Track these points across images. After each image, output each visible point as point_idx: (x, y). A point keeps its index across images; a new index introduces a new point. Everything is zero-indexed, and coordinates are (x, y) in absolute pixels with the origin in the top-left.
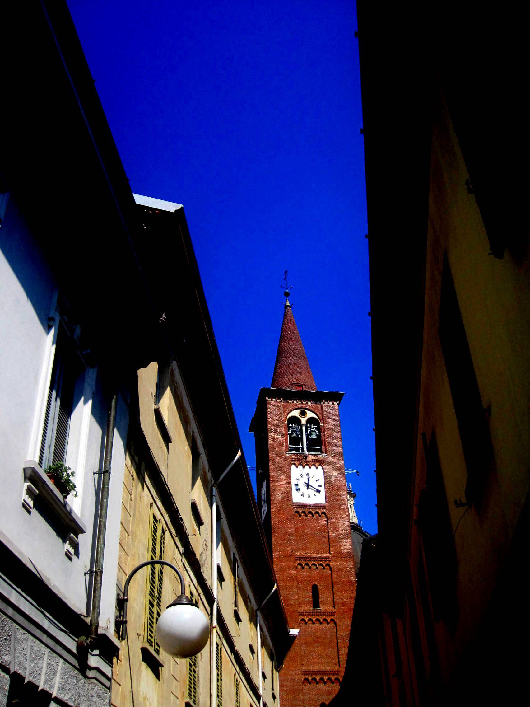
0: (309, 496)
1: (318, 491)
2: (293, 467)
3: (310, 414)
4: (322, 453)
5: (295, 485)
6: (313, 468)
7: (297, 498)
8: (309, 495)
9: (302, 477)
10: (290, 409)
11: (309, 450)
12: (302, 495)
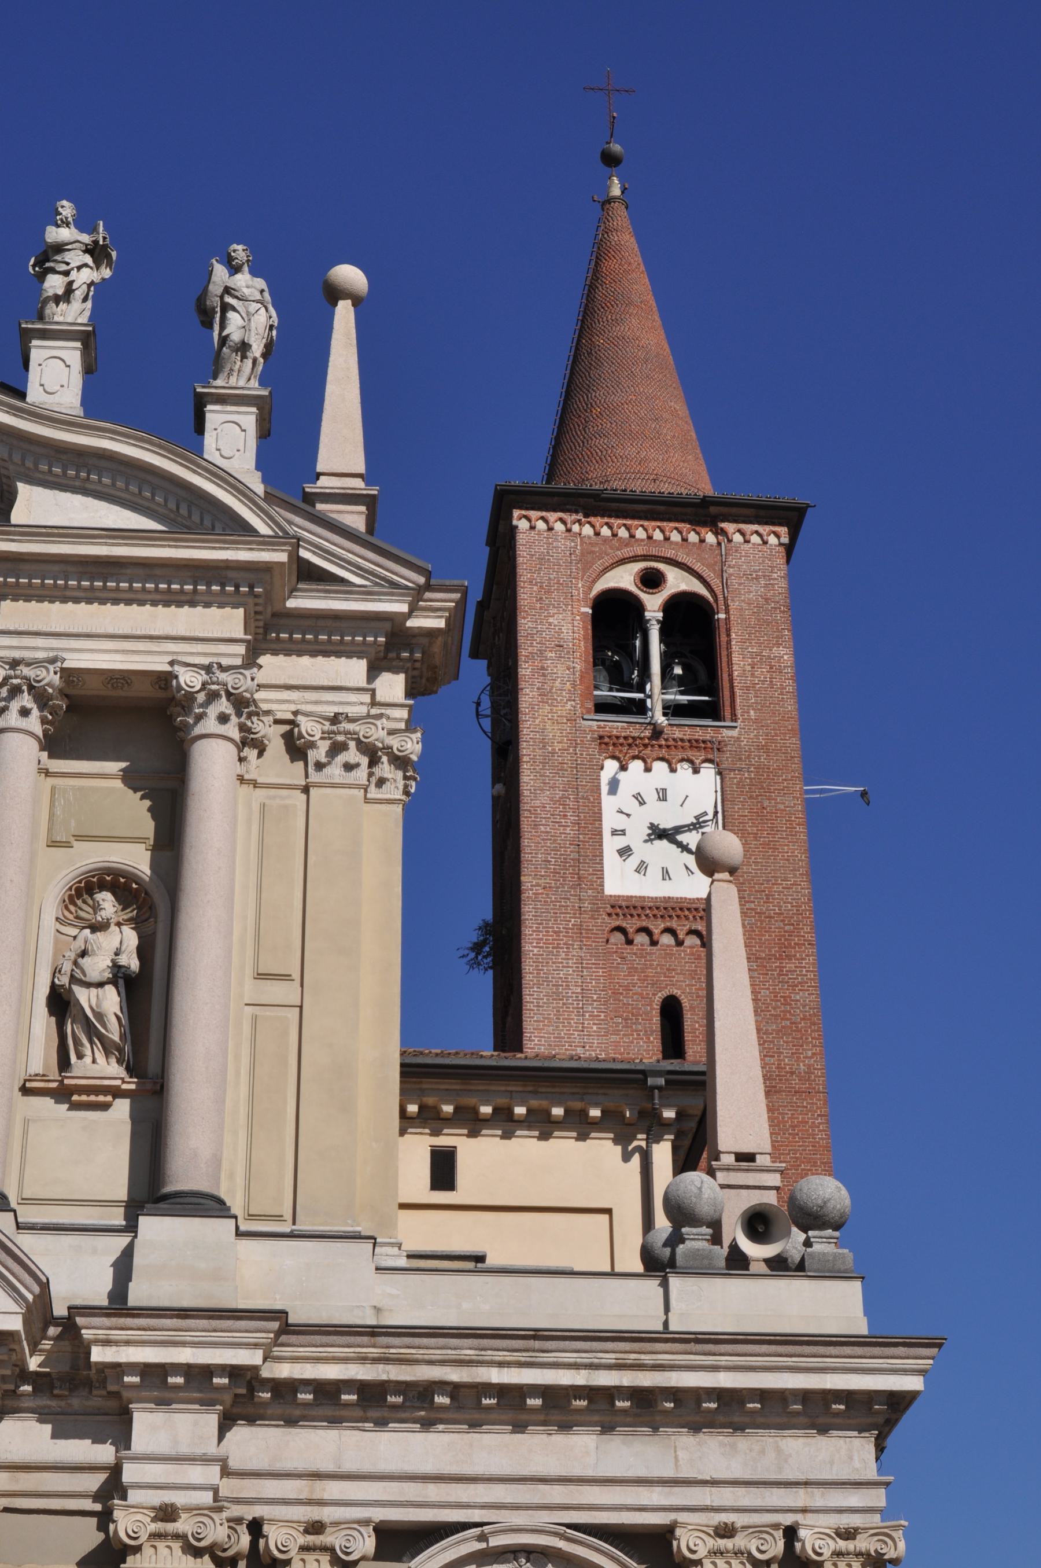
0: (666, 874)
3: (677, 582)
4: (719, 720)
5: (615, 833)
6: (684, 770)
8: (667, 872)
9: (642, 803)
10: (608, 561)
11: (673, 710)
12: (637, 871)
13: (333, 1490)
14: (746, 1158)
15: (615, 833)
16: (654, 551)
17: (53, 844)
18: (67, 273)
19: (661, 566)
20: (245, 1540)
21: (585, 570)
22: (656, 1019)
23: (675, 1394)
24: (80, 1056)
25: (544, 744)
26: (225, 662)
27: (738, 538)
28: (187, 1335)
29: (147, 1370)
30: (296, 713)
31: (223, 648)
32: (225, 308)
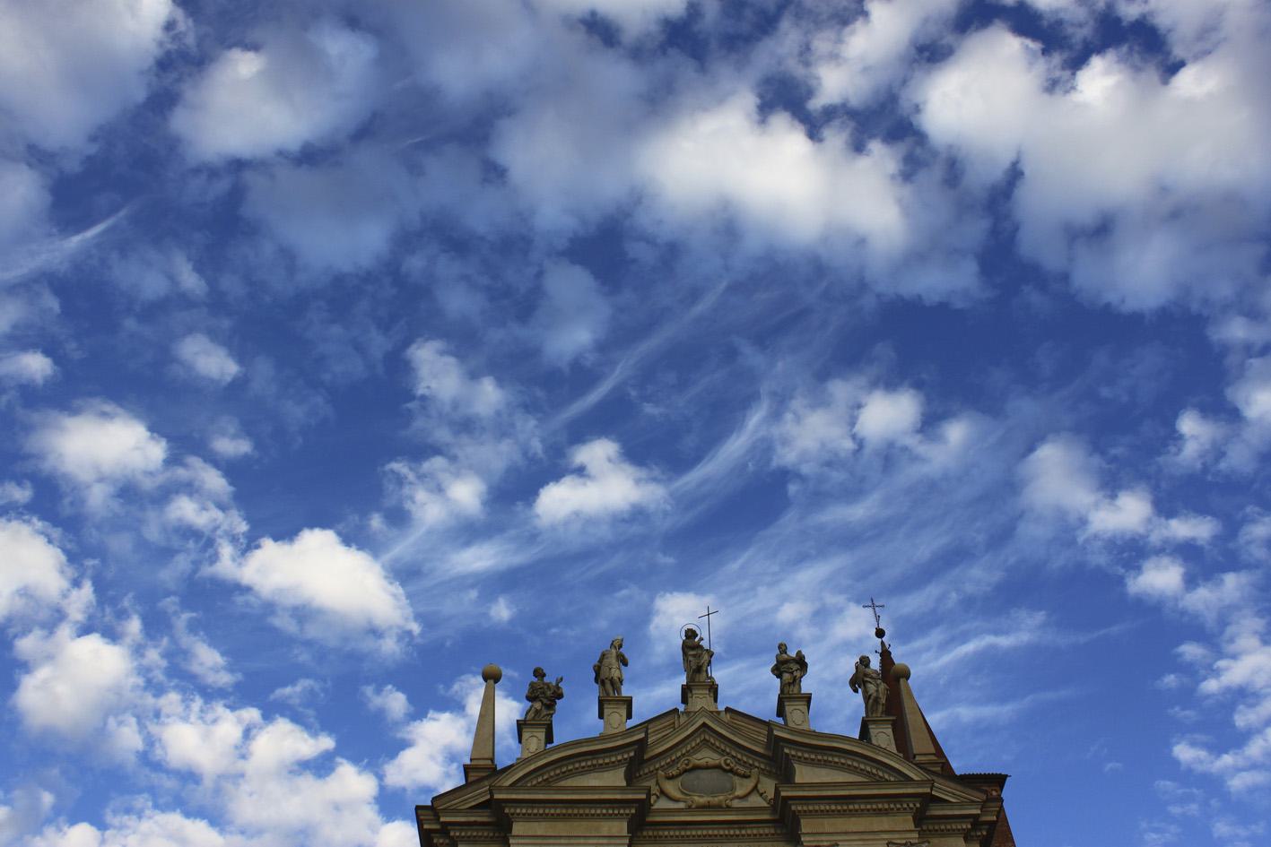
18: (792, 673)
31: (908, 835)
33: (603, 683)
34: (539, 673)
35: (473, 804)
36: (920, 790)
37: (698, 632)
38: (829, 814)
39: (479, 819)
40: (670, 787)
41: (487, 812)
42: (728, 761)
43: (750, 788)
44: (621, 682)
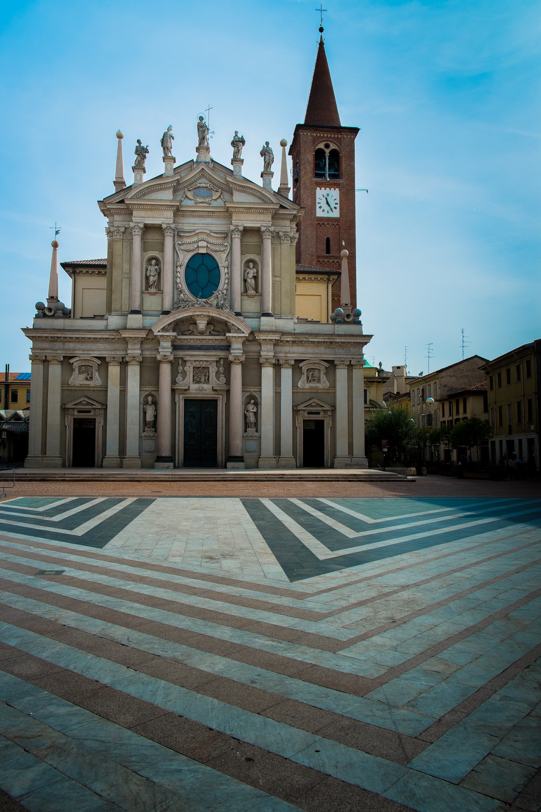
1: (335, 208)
2: (318, 188)
3: (333, 146)
5: (318, 203)
6: (332, 189)
7: (319, 213)
11: (331, 176)
13: (289, 355)
14: (346, 305)
15: (318, 203)
16: (328, 139)
17: (243, 254)
19: (329, 143)
20: (277, 362)
21: (314, 144)
22: (325, 242)
23: (336, 342)
24: (249, 290)
25: (305, 184)
26: (269, 225)
27: (345, 136)
28: (270, 335)
29: (263, 340)
30: (279, 231)
31: (268, 223)
32: (265, 154)
33: (164, 148)
34: (139, 141)
35: (118, 201)
36: (275, 207)
37: (204, 118)
38: (242, 212)
39: (121, 207)
40: (189, 194)
41: (123, 205)
42: (211, 186)
43: (218, 196)
44: (171, 148)
